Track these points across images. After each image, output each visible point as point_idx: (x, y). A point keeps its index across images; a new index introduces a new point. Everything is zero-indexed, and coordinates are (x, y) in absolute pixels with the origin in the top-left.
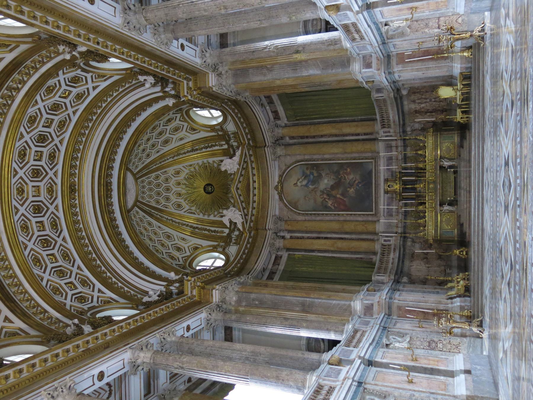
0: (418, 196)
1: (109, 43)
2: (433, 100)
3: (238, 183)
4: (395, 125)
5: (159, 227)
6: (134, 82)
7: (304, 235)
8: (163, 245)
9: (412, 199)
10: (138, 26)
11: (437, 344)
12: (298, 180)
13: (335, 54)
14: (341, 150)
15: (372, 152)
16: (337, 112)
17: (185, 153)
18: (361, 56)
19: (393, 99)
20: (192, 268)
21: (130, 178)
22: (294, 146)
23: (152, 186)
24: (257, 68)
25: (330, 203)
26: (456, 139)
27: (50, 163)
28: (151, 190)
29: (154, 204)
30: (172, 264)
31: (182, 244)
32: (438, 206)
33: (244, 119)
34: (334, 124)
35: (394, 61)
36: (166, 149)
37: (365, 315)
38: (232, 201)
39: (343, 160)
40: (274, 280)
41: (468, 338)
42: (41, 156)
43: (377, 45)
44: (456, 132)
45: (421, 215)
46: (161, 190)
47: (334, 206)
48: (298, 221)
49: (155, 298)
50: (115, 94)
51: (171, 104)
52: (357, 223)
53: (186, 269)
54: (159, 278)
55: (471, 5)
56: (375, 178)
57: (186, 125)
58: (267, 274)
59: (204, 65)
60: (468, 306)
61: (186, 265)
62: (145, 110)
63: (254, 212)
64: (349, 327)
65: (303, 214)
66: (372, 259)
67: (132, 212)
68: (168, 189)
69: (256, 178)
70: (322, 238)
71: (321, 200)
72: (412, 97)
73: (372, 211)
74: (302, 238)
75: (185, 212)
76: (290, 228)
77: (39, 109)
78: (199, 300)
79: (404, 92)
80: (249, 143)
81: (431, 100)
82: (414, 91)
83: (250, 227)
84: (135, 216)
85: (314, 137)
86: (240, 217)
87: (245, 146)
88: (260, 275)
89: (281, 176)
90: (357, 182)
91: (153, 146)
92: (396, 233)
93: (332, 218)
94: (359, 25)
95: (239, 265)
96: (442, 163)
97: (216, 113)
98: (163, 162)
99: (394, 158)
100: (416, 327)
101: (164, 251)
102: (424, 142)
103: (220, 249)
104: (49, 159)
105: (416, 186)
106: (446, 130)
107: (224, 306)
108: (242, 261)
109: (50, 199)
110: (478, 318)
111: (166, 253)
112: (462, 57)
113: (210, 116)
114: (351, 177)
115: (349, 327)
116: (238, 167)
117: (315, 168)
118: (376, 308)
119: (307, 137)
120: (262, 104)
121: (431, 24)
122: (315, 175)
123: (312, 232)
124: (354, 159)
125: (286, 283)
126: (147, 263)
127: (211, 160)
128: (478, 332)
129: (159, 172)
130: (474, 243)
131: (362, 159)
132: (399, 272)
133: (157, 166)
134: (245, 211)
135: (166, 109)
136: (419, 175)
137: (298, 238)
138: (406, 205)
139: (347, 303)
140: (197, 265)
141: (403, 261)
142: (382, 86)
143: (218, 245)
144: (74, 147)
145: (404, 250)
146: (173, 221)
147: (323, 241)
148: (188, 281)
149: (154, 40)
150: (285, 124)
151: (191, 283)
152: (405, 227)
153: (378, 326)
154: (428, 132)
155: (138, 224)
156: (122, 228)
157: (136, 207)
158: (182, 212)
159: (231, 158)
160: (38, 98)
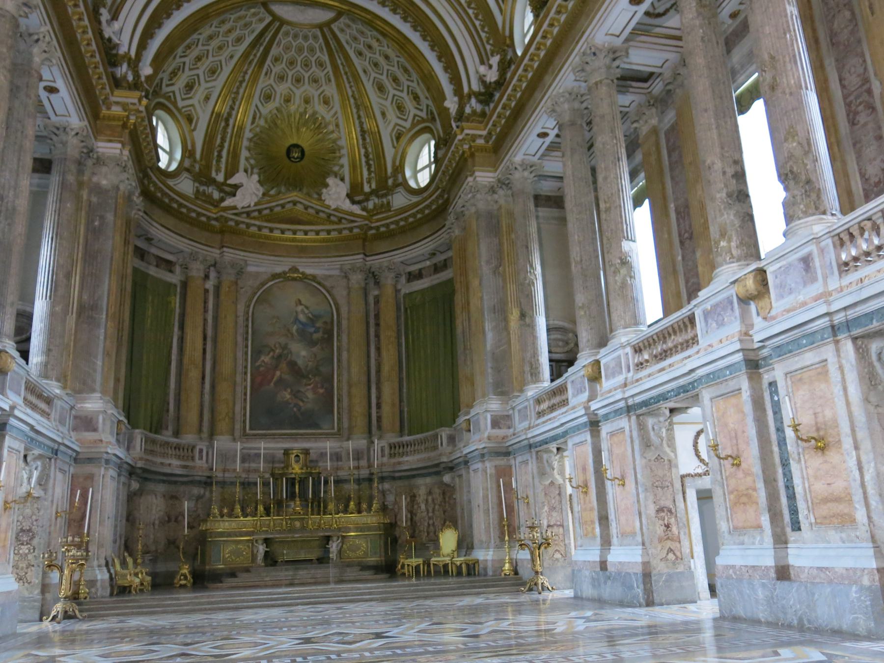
1: (563, 18)
3: (304, 205)
4: (394, 464)
5: (232, 57)
6: (488, 47)
8: (199, 59)
10: (588, 68)
11: (27, 544)
12: (307, 308)
13: (515, 371)
16: (417, 373)
17: (359, 117)
19: (436, 462)
21: (329, 15)
24: (500, 251)
25: (266, 359)
28: (300, 50)
29: (274, 51)
33: (412, 223)
34: (397, 368)
35: (501, 462)
37: (76, 417)
38: (272, 192)
39: (339, 381)
41: (40, 597)
43: (529, 436)
46: (299, 68)
48: (235, 303)
49: (108, 32)
50: (470, 12)
51: (447, 104)
54: (143, 46)
55: (587, 569)
57: (408, 125)
58: (141, 244)
60: (96, 593)
62: (439, 59)
63: (253, 229)
64: (54, 388)
65: (248, 313)
66: (167, 428)
68: (298, 80)
70: (205, 344)
73: (251, 429)
74: (206, 310)
75: (256, 106)
76: (224, 289)
78: (102, 115)
80: (371, 228)
82: (448, 492)
83: (227, 220)
85: (377, 336)
86: (245, 203)
87: (367, 222)
89: (314, 278)
90: (301, 404)
91: (376, 65)
93: (240, 362)
94: (564, 410)
97: (424, 179)
98: (348, 79)
99: (340, 463)
101: (187, 60)
103: (187, 164)
107: (90, 163)
110: (80, 611)
112: (502, 562)
113: (419, 168)
115: (54, 388)
116: (333, 207)
117: (326, 336)
118: (89, 436)
119: (377, 325)
120: (434, 254)
121: (554, 514)
122: (316, 336)
124: (339, 400)
127: (345, 161)
128: (53, 613)
130: (213, 596)
131: (339, 413)
133: (341, 67)
134: (256, 214)
137: (206, 302)
139: (98, 386)
143: (195, 161)
146: (241, 82)
147: (199, 346)
149: (561, 91)
150: (400, 290)
152: (223, 484)
153: (60, 440)
157: (271, 18)
158: (256, 100)
159: (348, 195)
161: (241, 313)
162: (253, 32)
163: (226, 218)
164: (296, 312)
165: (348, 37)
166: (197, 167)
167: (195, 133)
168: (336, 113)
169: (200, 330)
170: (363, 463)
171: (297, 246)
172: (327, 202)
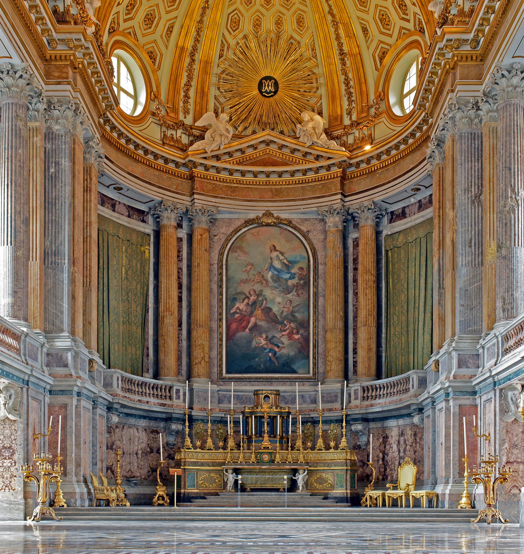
0: (250, 439)
20: (113, 48)
25: (241, 306)
30: (119, 4)
34: (375, 313)
39: (315, 327)
40: (100, 207)
44: (349, 491)
47: (236, 313)
52: (207, 349)
56: (282, 378)
73: (228, 372)
80: (351, 165)
90: (276, 349)
92: (191, 408)
96: (301, 472)
100: (34, 429)
102: (336, 447)
120: (418, 189)
122: (290, 283)
123: (189, 275)
124: (314, 346)
131: (314, 358)
140: (120, 59)
141: (144, 417)
143: (160, 103)
145: (162, 419)
164: (271, 259)
171: (271, 190)
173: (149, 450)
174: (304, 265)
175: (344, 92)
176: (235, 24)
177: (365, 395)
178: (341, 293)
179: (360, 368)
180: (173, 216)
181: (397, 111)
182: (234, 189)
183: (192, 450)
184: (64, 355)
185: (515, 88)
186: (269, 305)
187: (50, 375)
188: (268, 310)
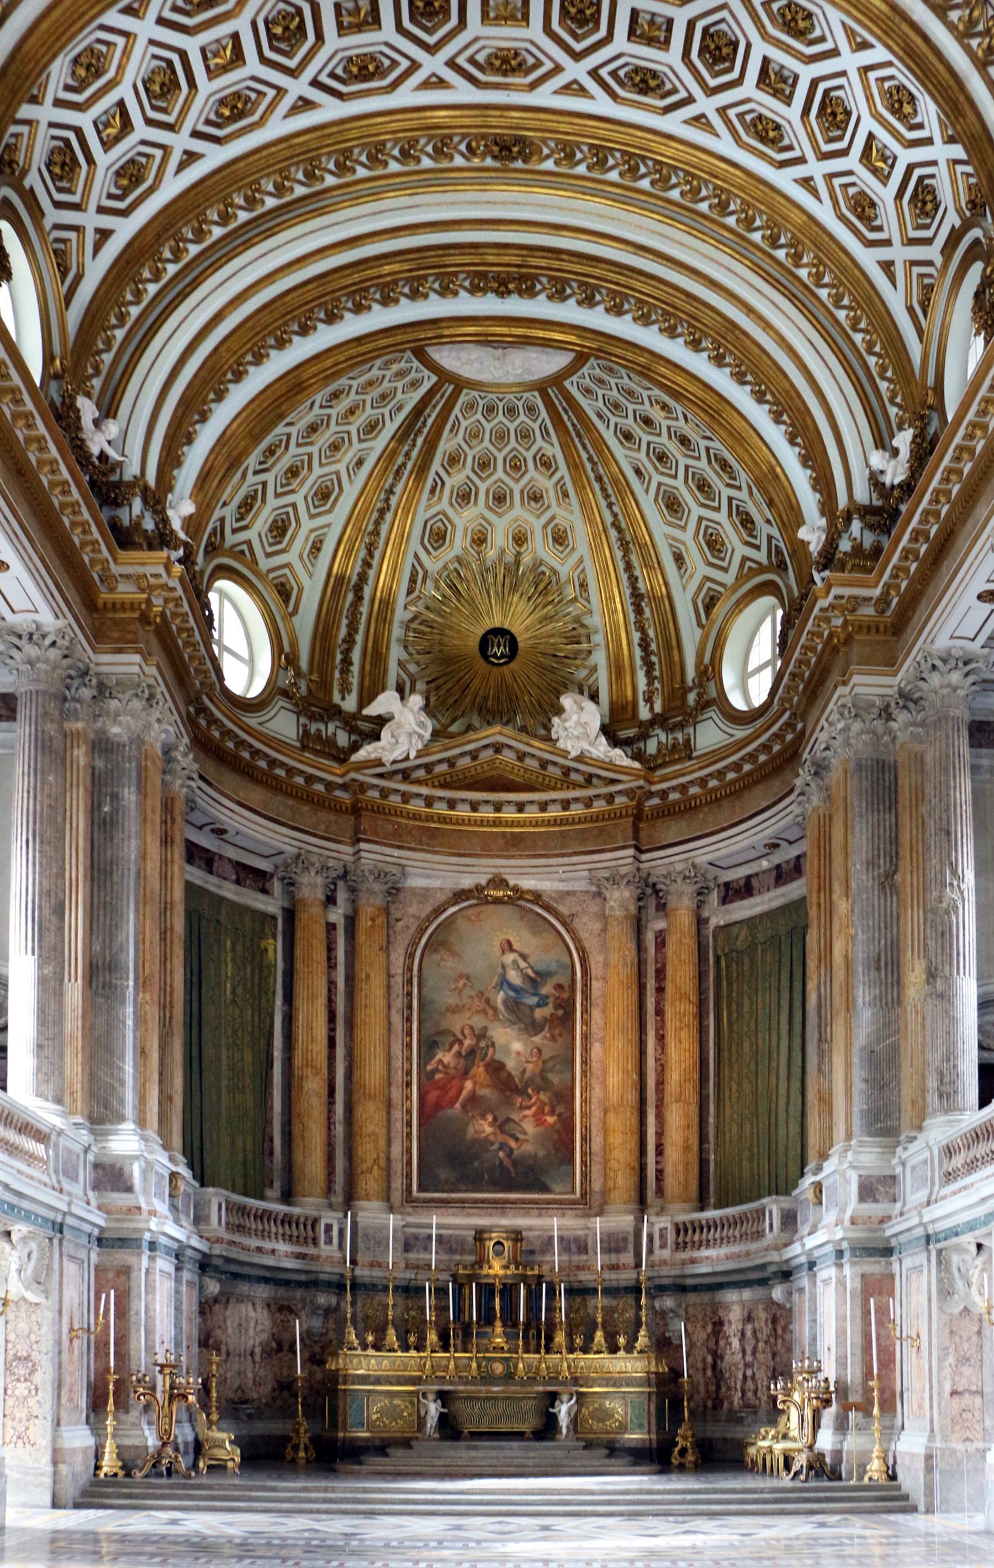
2: (749, 1372)
3: (517, 751)
4: (684, 1263)
5: (360, 463)
7: (341, 969)
9: (459, 1310)
14: (614, 1097)
15: (605, 1192)
16: (734, 1087)
17: (629, 567)
18: (899, 1170)
22: (633, 946)
23: (513, 443)
26: (634, 1437)
27: (621, 73)
28: (501, 436)
29: (446, 445)
31: (300, 543)
32: (436, 1388)
34: (696, 1076)
36: (648, 502)
38: (454, 728)
39: (584, 1101)
40: (188, 868)
42: (650, 41)
44: (654, 1436)
45: (411, 1335)
46: (500, 474)
48: (386, 950)
52: (382, 1142)
53: (209, 556)
56: (523, 1201)
59: (923, 666)
61: (223, 555)
63: (416, 806)
65: (411, 969)
66: (271, 1185)
67: (416, 363)
68: (500, 499)
69: (532, 813)
70: (332, 1030)
71: (456, 1029)
72: (762, 1315)
73: (421, 1188)
74: (332, 966)
76: (364, 923)
77: (835, 53)
79: (777, 1293)
80: (651, 795)
81: (747, 1365)
84: (401, 374)
85: (659, 1012)
86: (398, 754)
87: (641, 782)
88: (198, 818)
90: (513, 1144)
95: (231, 745)
97: (760, 689)
98: (603, 489)
99: (584, 1257)
101: (269, 477)
104: (637, 70)
105: (498, 1323)
106: (660, 1408)
108: (246, 755)
109: (472, 60)
111: (264, 484)
114: (530, 1127)
116: (574, 754)
124: (584, 1139)
125: (180, 908)
126: (223, 415)
127: (600, 658)
129: (563, 470)
131: (583, 1163)
132: (233, 1268)
133: (588, 466)
134: (421, 773)
135: (791, 516)
136: (533, 1331)
137: (330, 949)
138: (441, 1292)
141: (266, 1280)
142: (804, 1229)
143: (298, 674)
144: (676, 168)
145: (300, 1284)
146: (382, 512)
148: (168, 566)
150: (707, 921)
151: (157, 576)
154: (658, 1360)
155: (370, 383)
156: (352, 326)
157: (434, 379)
158: (415, 545)
159: (606, 730)
160: (879, 54)
161: (398, 967)
162: (400, 408)
163: (362, 784)
165: (600, 403)
166: (303, 685)
167: (295, 620)
168: (581, 560)
169: (322, 1001)
170: (627, 1258)
172: (561, 744)
173: (274, 1345)
174: (565, 981)
175: (639, 662)
176: (438, 537)
177: (680, 1240)
178: (634, 1036)
179: (670, 1183)
180: (319, 880)
181: (737, 702)
182: (433, 834)
183: (359, 1352)
184: (126, 1170)
185: (955, 689)
186: (498, 1057)
187: (99, 1208)
188: (496, 1068)
